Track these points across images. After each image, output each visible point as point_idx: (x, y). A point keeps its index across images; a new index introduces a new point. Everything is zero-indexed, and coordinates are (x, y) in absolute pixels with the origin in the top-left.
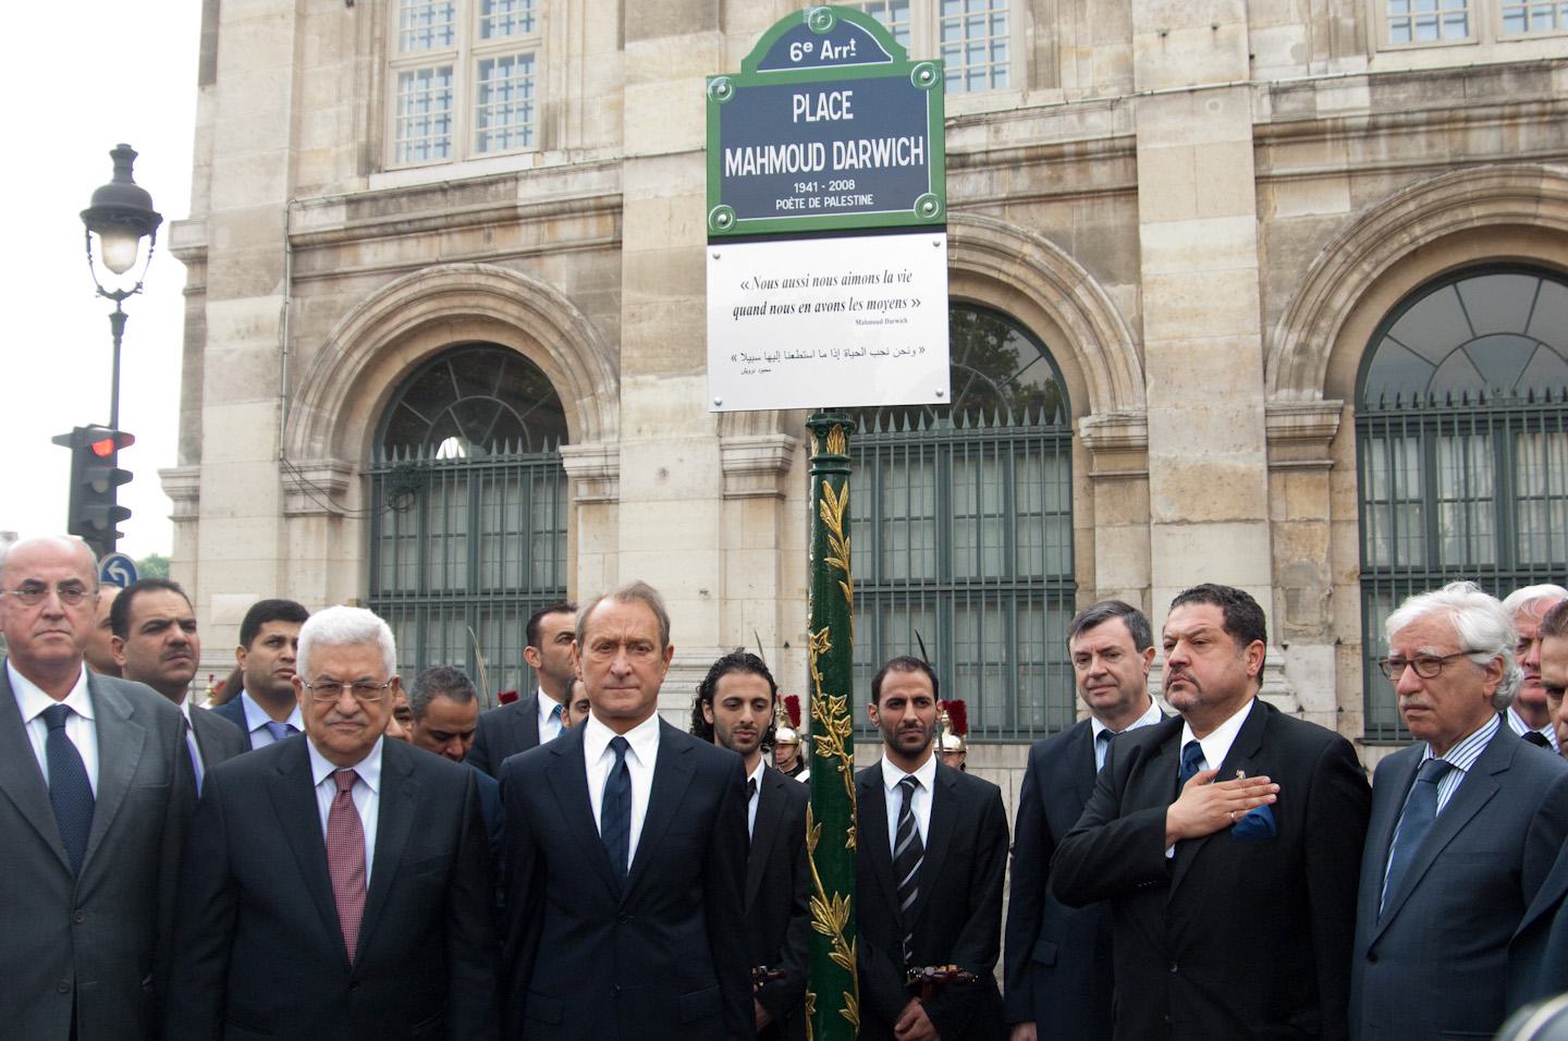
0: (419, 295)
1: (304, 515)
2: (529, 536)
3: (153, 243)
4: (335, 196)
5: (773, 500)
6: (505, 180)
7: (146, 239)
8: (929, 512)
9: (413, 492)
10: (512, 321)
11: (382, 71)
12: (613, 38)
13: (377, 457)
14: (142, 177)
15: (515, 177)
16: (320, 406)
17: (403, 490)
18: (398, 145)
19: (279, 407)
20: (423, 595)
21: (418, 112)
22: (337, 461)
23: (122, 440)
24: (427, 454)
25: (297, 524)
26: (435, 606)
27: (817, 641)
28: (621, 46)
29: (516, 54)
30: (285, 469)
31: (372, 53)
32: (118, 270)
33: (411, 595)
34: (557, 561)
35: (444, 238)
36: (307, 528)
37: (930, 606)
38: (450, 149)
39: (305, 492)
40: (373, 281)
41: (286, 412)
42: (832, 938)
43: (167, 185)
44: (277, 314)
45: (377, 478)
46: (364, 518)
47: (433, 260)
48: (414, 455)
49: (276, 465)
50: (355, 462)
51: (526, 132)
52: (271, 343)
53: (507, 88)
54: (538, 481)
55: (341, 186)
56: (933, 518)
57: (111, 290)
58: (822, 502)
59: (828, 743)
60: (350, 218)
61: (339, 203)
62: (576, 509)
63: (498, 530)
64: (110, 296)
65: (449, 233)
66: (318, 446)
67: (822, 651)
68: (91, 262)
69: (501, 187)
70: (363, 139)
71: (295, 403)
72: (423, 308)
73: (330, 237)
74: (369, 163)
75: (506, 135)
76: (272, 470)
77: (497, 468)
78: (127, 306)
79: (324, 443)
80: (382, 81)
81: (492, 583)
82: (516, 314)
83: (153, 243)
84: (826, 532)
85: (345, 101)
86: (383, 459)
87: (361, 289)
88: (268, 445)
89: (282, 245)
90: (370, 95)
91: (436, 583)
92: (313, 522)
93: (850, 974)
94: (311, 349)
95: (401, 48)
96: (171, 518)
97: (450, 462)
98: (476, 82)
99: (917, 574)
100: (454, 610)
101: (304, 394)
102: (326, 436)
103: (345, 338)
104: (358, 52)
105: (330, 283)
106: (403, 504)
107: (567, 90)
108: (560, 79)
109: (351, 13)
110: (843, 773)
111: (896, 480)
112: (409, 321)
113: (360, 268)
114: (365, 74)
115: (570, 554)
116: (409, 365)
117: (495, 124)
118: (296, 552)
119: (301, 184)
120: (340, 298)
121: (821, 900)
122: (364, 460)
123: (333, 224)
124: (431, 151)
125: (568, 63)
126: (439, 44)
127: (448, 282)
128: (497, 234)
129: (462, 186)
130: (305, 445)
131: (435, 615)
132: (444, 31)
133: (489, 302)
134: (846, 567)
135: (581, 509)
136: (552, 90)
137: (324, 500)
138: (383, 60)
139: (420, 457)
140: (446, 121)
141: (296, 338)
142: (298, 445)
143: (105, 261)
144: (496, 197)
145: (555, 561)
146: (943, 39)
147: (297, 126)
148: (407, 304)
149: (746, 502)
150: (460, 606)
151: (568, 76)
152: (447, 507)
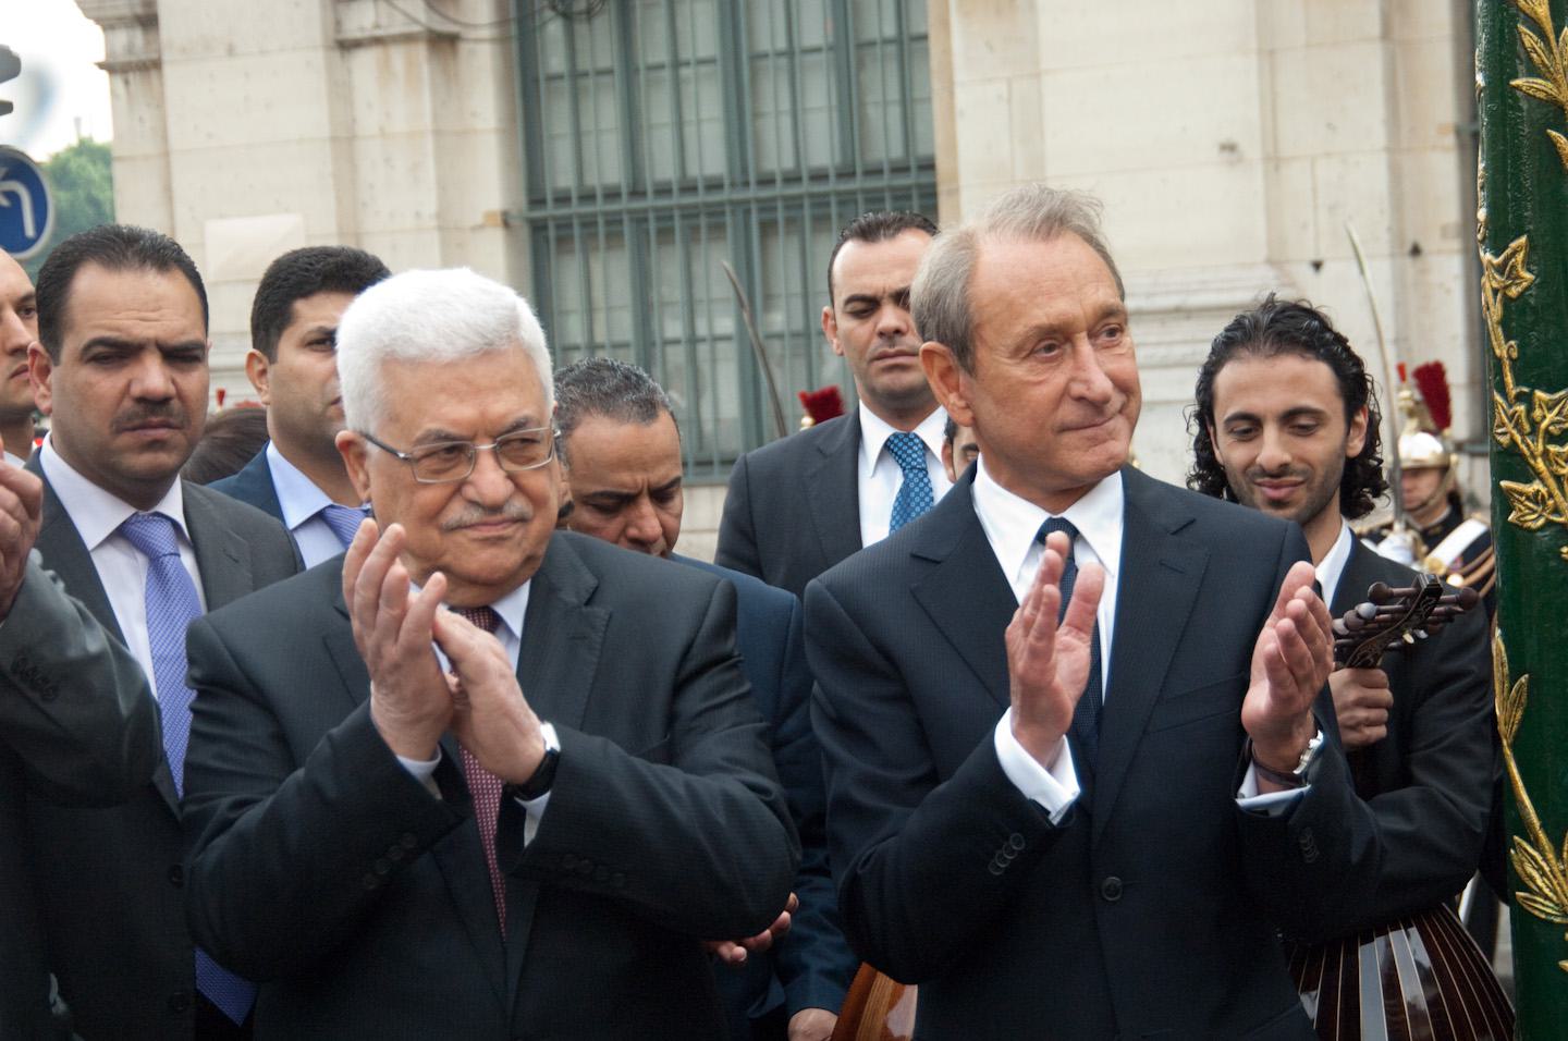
1: (378, 41)
25: (365, 62)
26: (664, 216)
27: (1501, 269)
33: (612, 194)
36: (385, 67)
46: (502, 41)
59: (1536, 498)
63: (782, 44)
67: (1514, 292)
81: (777, 156)
84: (1514, 19)
92: (398, 55)
96: (101, 66)
100: (703, 221)
150: (715, 211)
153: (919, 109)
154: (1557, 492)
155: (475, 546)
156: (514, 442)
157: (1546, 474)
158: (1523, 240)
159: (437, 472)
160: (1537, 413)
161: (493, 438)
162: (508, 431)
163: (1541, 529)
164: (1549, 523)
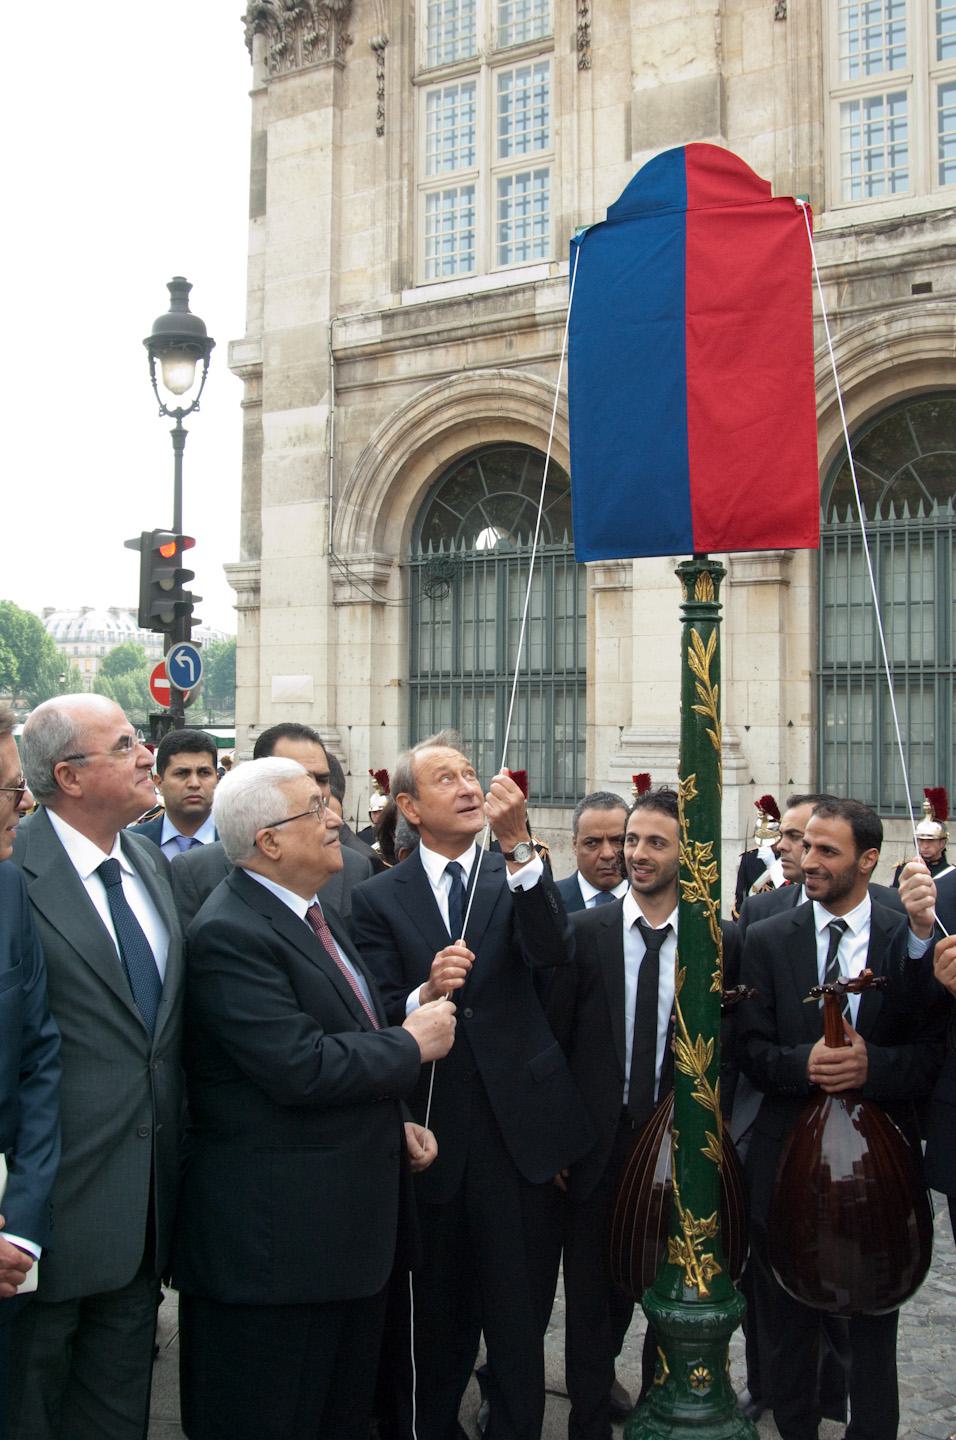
0: (448, 401)
1: (351, 604)
2: (552, 621)
3: (206, 365)
4: (372, 312)
5: (777, 587)
6: (524, 290)
7: (201, 362)
8: (928, 597)
9: (447, 583)
10: (532, 421)
11: (411, 193)
12: (621, 147)
13: (414, 551)
14: (197, 306)
15: (533, 287)
16: (363, 504)
17: (437, 580)
18: (427, 261)
19: (327, 507)
20: (457, 675)
21: (444, 230)
22: (379, 555)
23: (184, 543)
24: (470, 545)
25: (345, 611)
26: (468, 686)
27: (684, 787)
28: (628, 157)
29: (532, 169)
30: (332, 563)
31: (401, 177)
32: (178, 392)
33: (446, 675)
34: (576, 643)
35: (470, 347)
36: (354, 614)
37: (929, 687)
38: (475, 263)
39: (350, 582)
40: (407, 388)
41: (333, 511)
42: (695, 1079)
43: (220, 312)
44: (325, 423)
45: (414, 569)
46: (404, 606)
47: (460, 367)
48: (447, 548)
49: (326, 556)
50: (394, 555)
51: (543, 244)
52: (318, 448)
53: (525, 203)
54: (559, 570)
55: (377, 302)
56: (932, 603)
57: (171, 408)
58: (690, 649)
60: (385, 332)
61: (375, 318)
62: (594, 595)
64: (172, 414)
65: (474, 342)
66: (362, 541)
67: (689, 798)
68: (155, 385)
69: (520, 297)
70: (395, 258)
71: (340, 503)
72: (452, 412)
73: (368, 349)
74: (402, 280)
75: (524, 248)
76: (323, 563)
77: (522, 559)
78: (186, 422)
79: (367, 538)
80: (411, 203)
82: (536, 415)
83: (206, 365)
85: (379, 224)
86: (420, 552)
87: (397, 396)
88: (317, 542)
89: (326, 359)
90: (401, 217)
91: (469, 665)
92: (359, 610)
93: (711, 1115)
94: (353, 453)
95: (428, 172)
96: (235, 608)
97: (480, 554)
98: (496, 199)
99: (916, 656)
100: (484, 689)
101: (349, 494)
102: (369, 532)
103: (383, 442)
104: (388, 178)
105: (369, 392)
106: (438, 593)
107: (579, 201)
108: (572, 191)
109: (381, 141)
110: (708, 918)
111: (897, 564)
112: (440, 424)
113: (397, 377)
114: (396, 197)
115: (588, 638)
116: (441, 465)
117: (514, 238)
118: (344, 638)
119: (342, 303)
120: (379, 406)
121: (685, 1042)
122: (403, 552)
123: (371, 338)
124: (457, 266)
125: (579, 175)
126: (462, 164)
127: (475, 387)
128: (518, 340)
129: (485, 297)
130: (350, 541)
131: (467, 694)
132: (466, 152)
133: (512, 405)
134: (714, 715)
135: (598, 596)
136: (565, 202)
137: (368, 590)
138: (411, 183)
139: (453, 550)
140: (470, 236)
141: (342, 443)
142: (344, 540)
143: (166, 384)
144: (516, 306)
145: (576, 644)
146: (941, 129)
147: (337, 248)
148: (438, 409)
149: (751, 588)
150: (489, 686)
151: (579, 188)
152: (478, 595)
153: (580, 647)
154: (702, 887)
157: (698, 879)
158: (694, 775)
160: (696, 852)
163: (696, 902)
164: (699, 901)
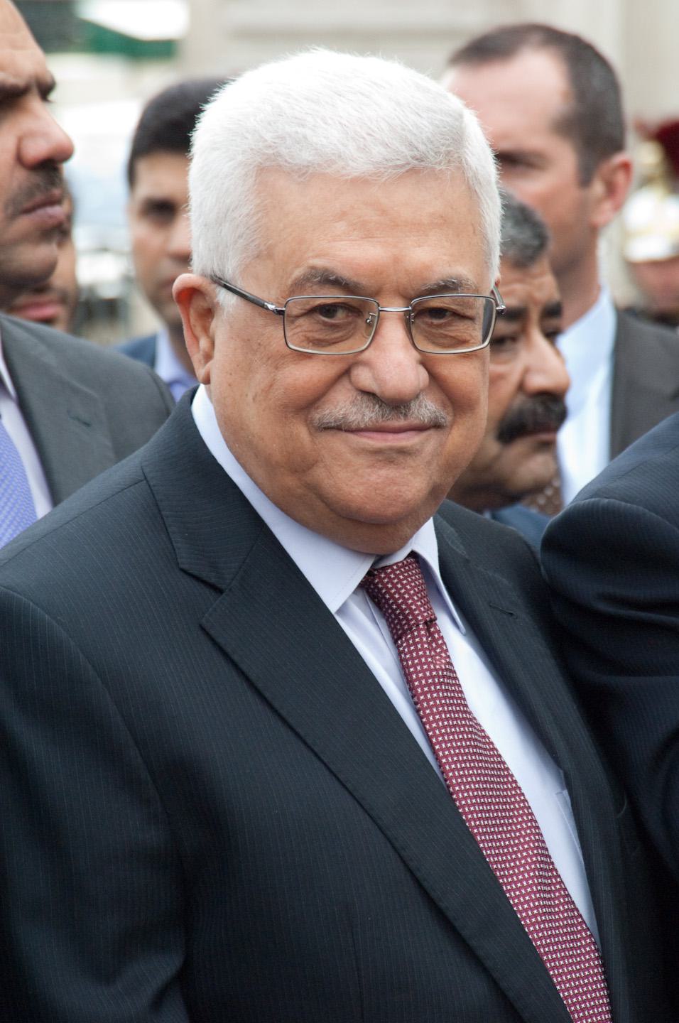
155: (361, 461)
156: (432, 311)
159: (318, 343)
161: (408, 298)
162: (432, 292)
